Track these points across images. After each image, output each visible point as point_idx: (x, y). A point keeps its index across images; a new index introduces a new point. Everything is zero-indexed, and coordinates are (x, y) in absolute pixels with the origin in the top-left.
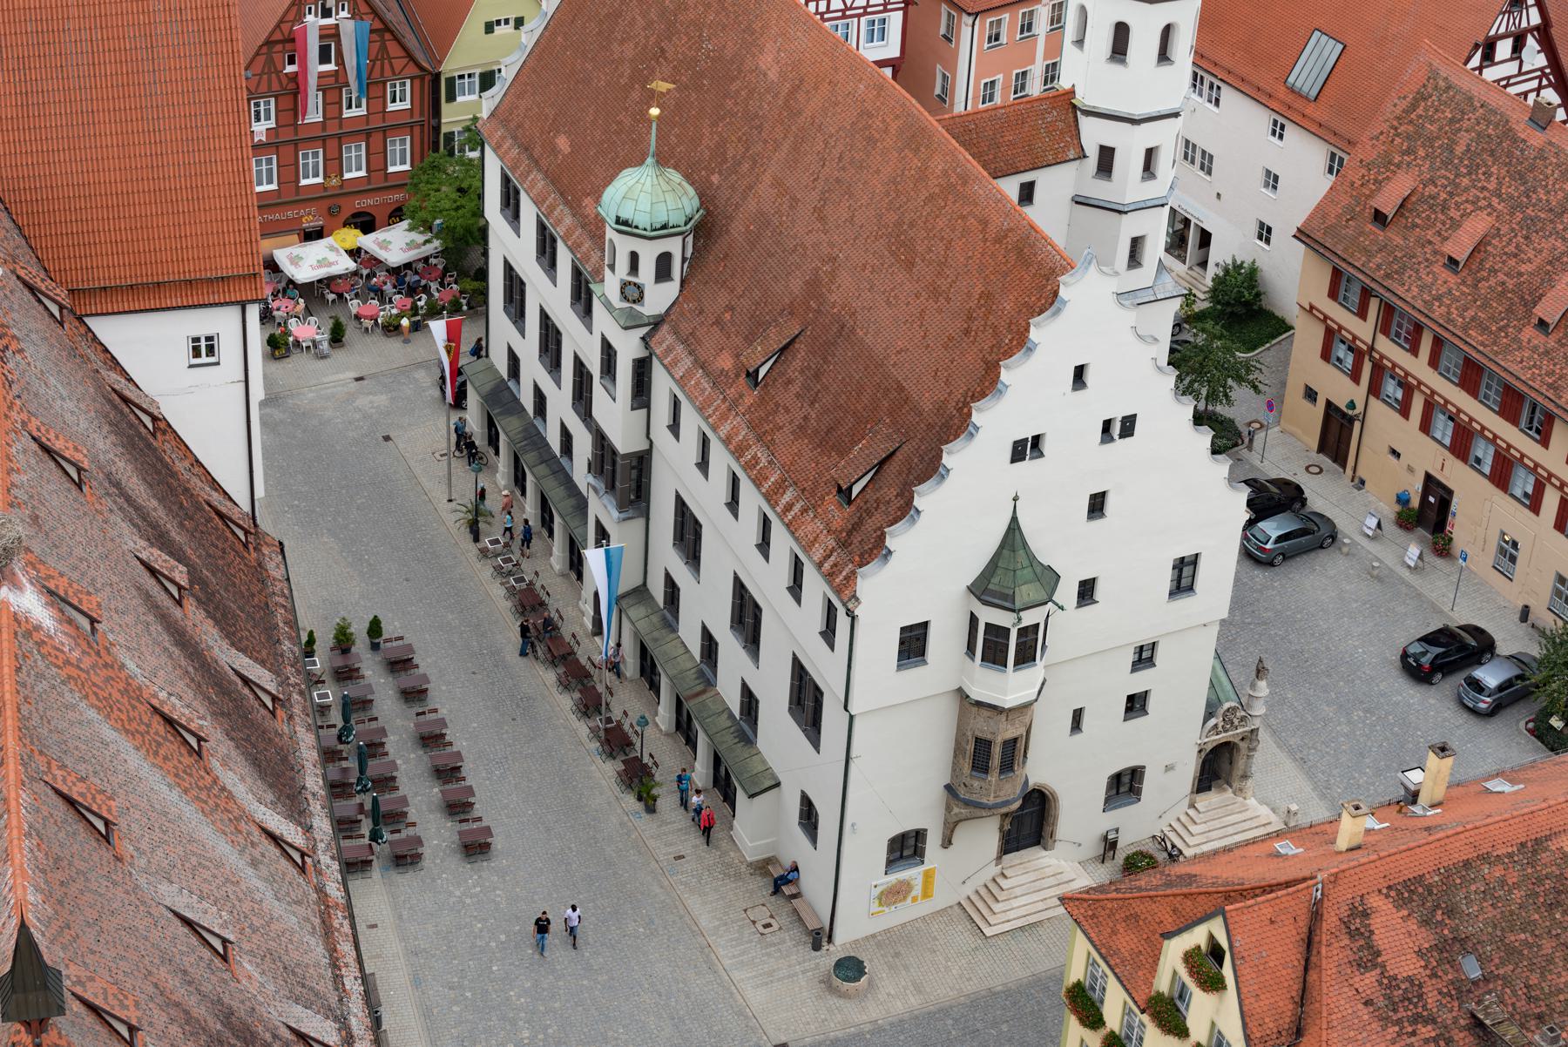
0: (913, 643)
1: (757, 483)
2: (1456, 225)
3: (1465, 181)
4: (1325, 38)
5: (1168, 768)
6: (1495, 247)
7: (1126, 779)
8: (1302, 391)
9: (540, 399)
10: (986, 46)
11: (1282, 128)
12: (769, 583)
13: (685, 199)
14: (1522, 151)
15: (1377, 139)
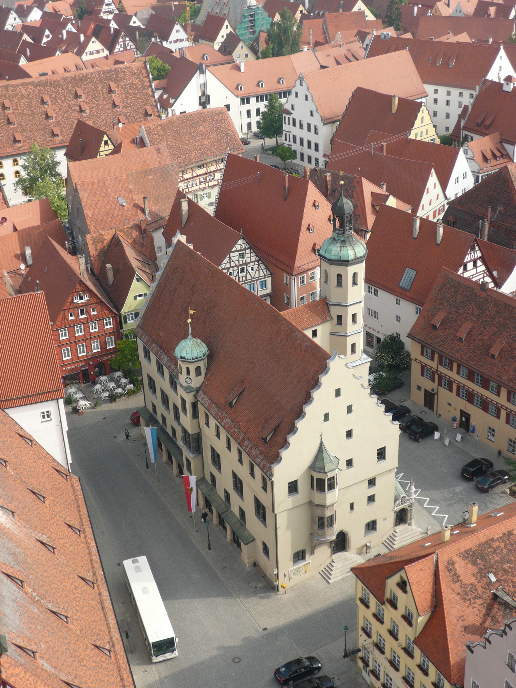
0: (293, 487)
2: (460, 326)
3: (461, 311)
4: (410, 270)
5: (385, 519)
6: (474, 332)
7: (371, 524)
8: (416, 388)
9: (164, 418)
10: (300, 285)
11: (400, 301)
12: (243, 472)
13: (202, 348)
15: (431, 301)
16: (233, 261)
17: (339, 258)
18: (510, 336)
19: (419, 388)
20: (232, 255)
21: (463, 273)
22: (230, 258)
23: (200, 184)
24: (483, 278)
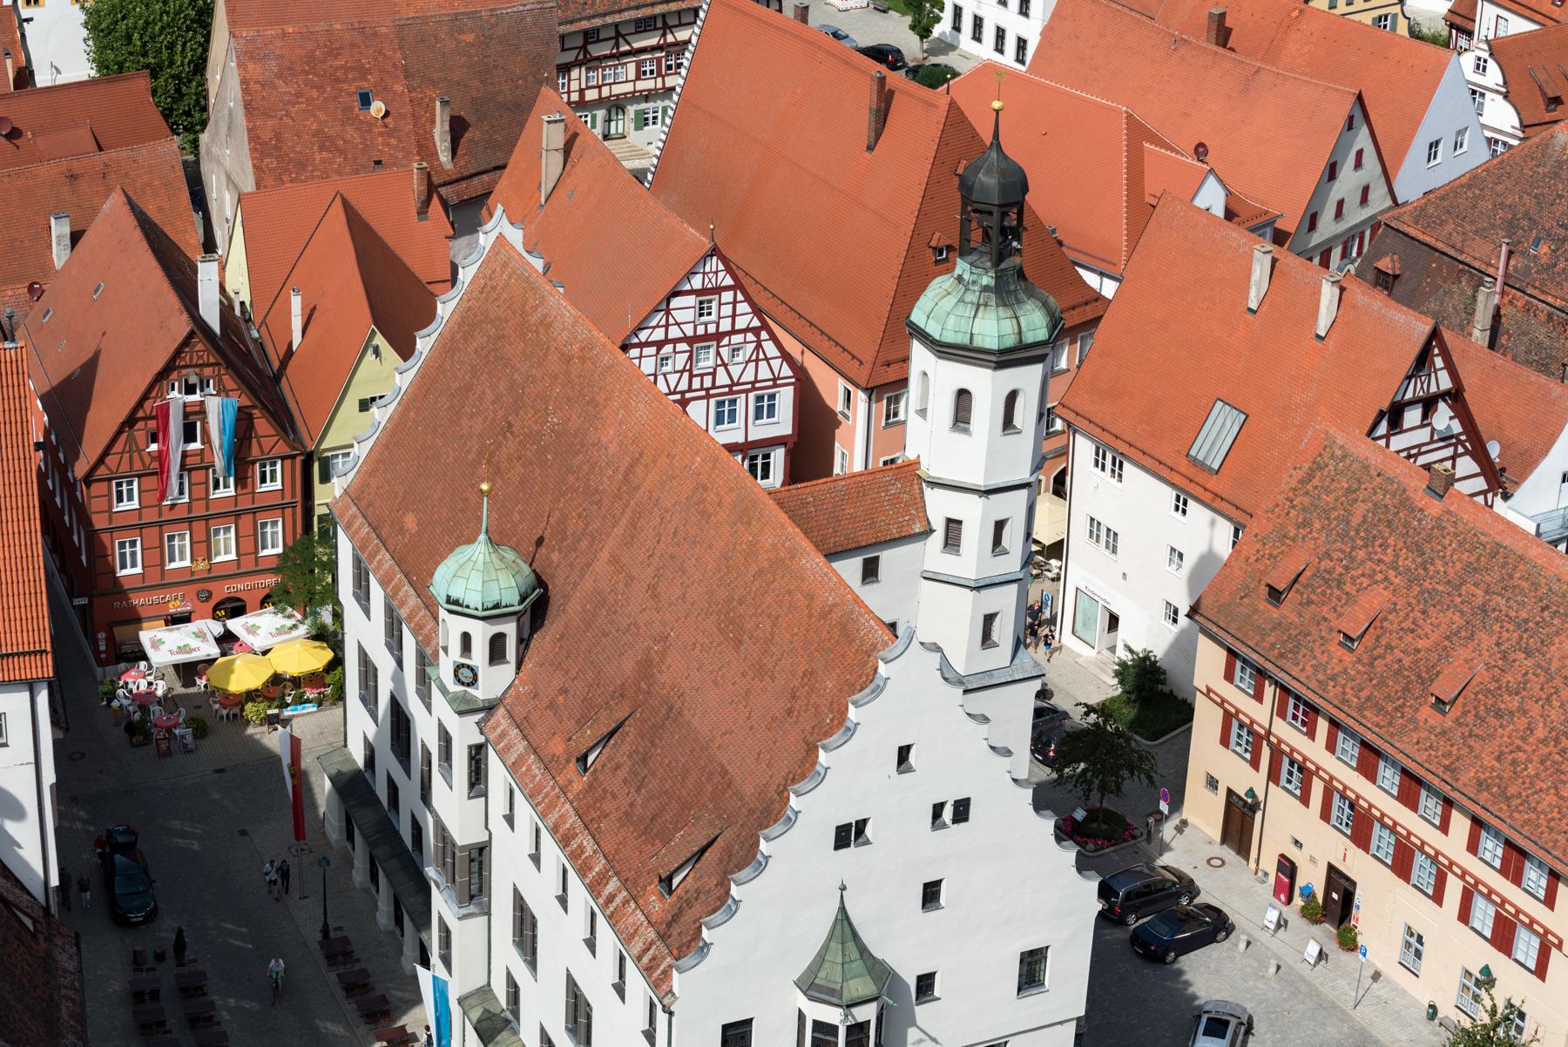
1: (582, 872)
2: (1350, 599)
3: (1361, 554)
8: (1203, 779)
11: (1185, 503)
14: (1420, 521)
16: (678, 324)
17: (966, 341)
18: (1498, 644)
19: (1212, 783)
20: (676, 302)
21: (1387, 437)
22: (668, 312)
23: (638, 78)
24: (1453, 458)
